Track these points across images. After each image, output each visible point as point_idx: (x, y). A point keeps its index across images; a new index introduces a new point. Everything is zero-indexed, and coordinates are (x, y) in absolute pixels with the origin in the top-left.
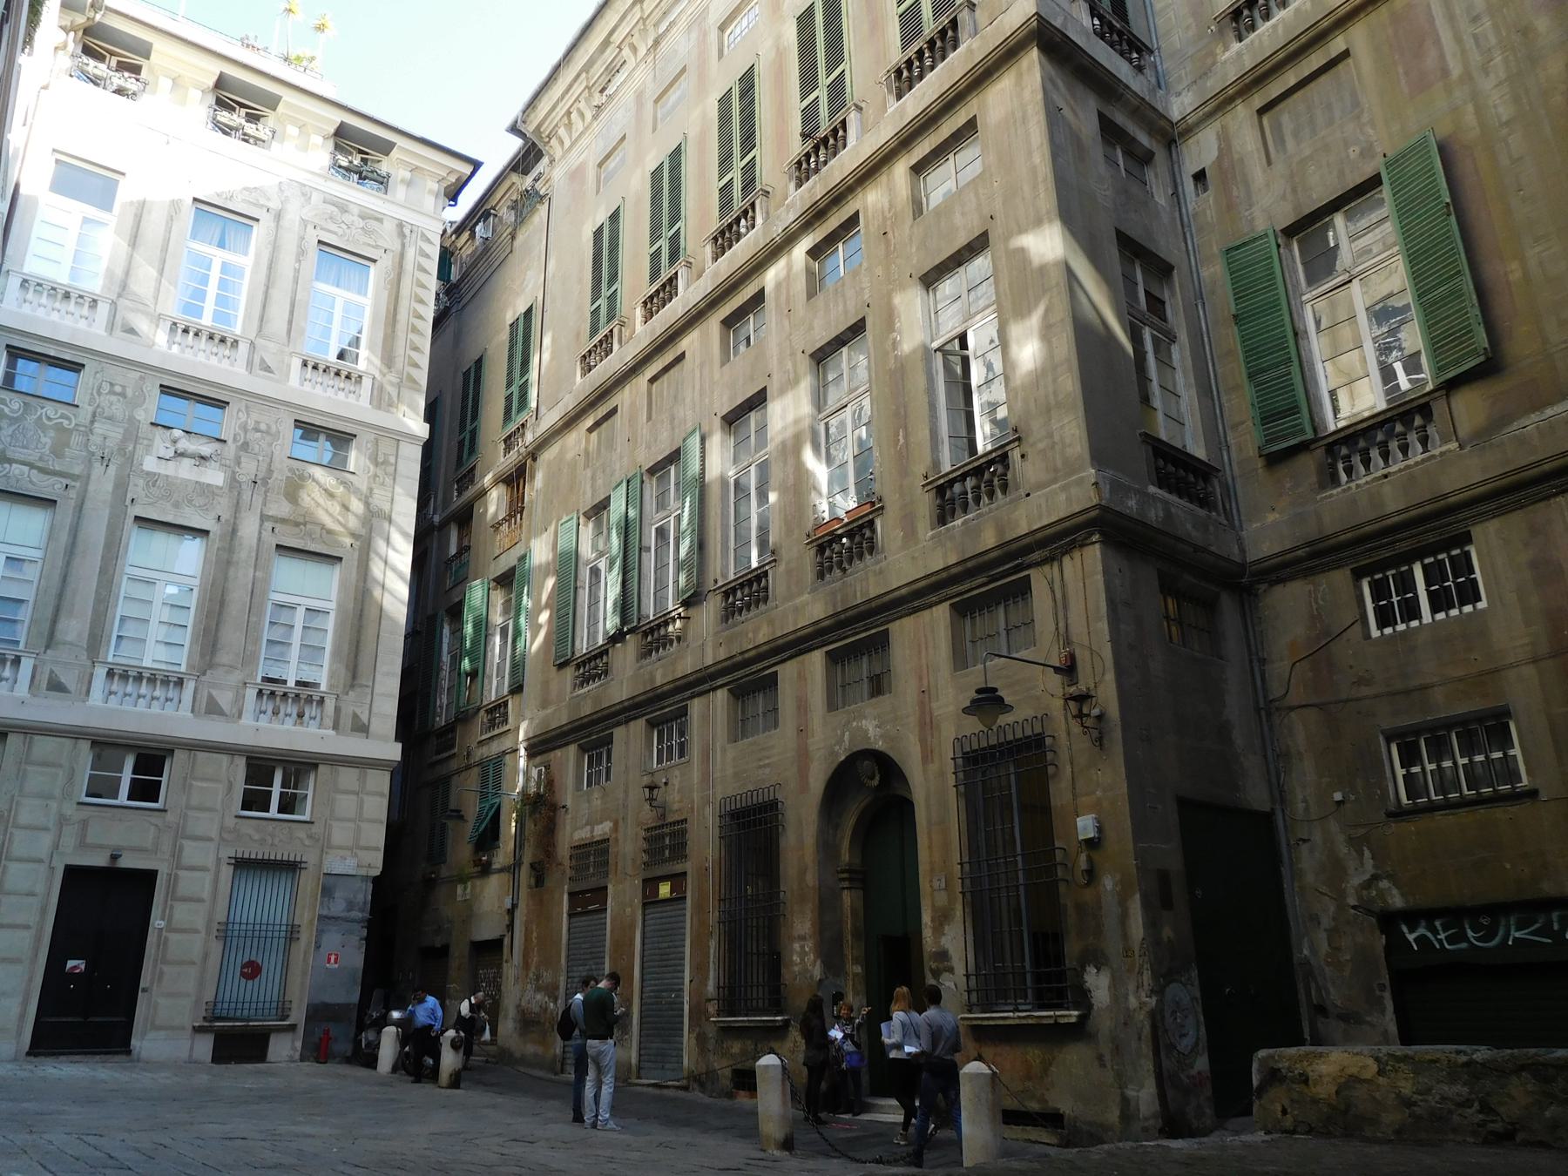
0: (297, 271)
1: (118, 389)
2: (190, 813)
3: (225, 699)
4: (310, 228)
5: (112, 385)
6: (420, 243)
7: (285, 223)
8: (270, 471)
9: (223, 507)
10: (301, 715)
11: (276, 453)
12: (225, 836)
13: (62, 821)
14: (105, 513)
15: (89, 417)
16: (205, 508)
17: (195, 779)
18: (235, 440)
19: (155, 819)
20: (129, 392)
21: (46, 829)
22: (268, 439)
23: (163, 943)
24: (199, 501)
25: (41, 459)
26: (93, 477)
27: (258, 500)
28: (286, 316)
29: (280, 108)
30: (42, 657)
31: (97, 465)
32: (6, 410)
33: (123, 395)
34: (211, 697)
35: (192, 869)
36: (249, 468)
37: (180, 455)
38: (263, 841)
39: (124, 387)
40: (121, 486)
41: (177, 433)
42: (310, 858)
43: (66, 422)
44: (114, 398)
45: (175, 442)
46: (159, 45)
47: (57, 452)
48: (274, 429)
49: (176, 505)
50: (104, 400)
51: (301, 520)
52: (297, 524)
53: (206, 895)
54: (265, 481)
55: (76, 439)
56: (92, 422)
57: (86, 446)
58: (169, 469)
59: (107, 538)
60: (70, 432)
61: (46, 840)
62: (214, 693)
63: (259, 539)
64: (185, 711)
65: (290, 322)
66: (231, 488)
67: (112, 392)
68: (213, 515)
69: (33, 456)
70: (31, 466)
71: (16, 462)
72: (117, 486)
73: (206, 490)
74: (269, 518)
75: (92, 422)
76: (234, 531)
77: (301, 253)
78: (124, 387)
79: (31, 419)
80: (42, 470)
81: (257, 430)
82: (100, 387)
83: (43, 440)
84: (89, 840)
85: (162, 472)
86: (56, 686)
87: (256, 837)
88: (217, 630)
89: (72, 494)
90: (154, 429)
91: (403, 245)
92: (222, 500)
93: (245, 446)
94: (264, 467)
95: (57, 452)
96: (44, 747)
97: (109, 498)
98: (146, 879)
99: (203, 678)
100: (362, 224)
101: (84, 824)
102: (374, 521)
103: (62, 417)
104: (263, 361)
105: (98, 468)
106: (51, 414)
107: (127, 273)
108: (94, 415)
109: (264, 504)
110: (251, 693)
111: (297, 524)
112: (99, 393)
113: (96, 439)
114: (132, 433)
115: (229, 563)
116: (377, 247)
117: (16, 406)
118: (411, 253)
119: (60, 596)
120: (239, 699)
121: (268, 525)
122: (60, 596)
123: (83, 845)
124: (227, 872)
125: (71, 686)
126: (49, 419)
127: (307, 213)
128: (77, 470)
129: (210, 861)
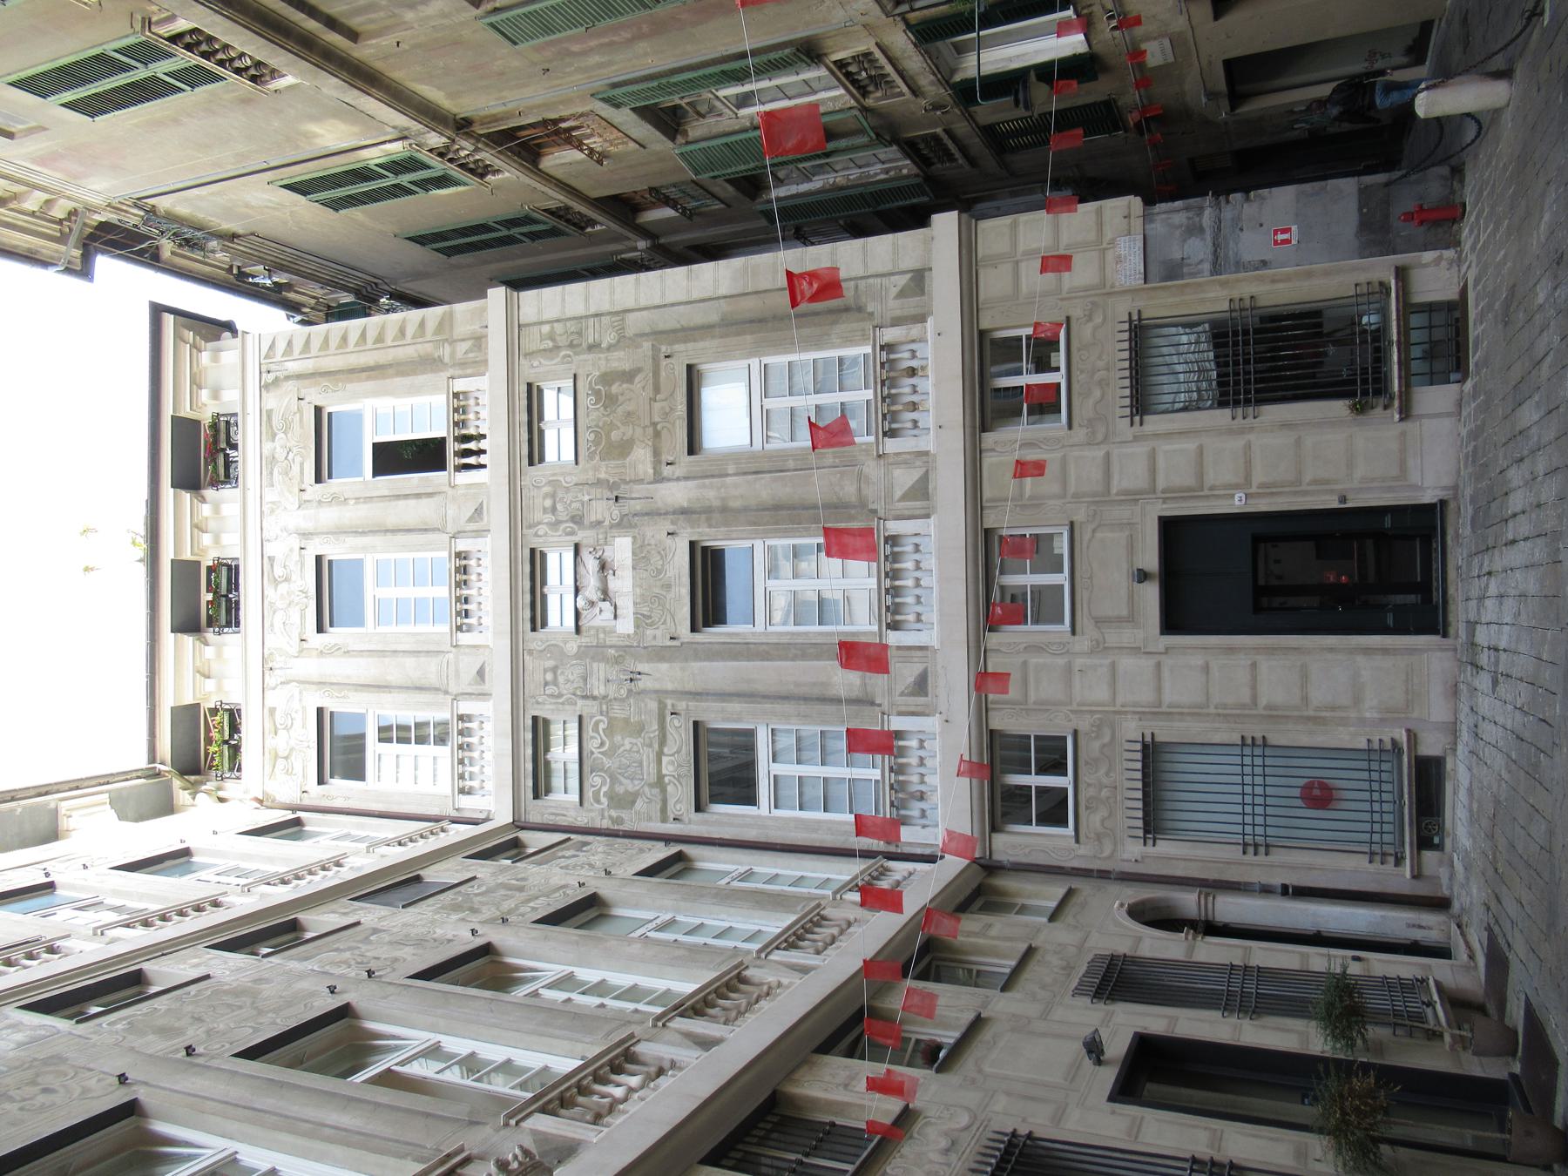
1: (549, 677)
2: (1072, 489)
3: (905, 478)
5: (546, 684)
6: (278, 358)
8: (599, 483)
9: (656, 531)
10: (912, 372)
11: (575, 480)
12: (1100, 437)
13: (1100, 648)
14: (696, 666)
17: (1021, 495)
18: (572, 533)
19: (1084, 536)
20: (550, 663)
21: (1113, 666)
22: (560, 494)
23: (1269, 489)
24: (656, 560)
25: (650, 746)
26: (657, 686)
27: (639, 490)
28: (412, 502)
29: (187, 556)
30: (885, 708)
31: (641, 685)
32: (605, 789)
33: (554, 670)
34: (904, 498)
35: (1153, 471)
36: (602, 510)
37: (606, 595)
38: (1103, 384)
40: (659, 654)
41: (581, 603)
42: (1122, 309)
43: (602, 726)
44: (561, 679)
45: (592, 604)
46: (168, 701)
47: (640, 729)
48: (547, 489)
49: (668, 587)
50: (566, 689)
51: (650, 430)
52: (657, 434)
53: (1190, 445)
54: (612, 486)
55: (618, 712)
56: (595, 698)
57: (623, 700)
58: (627, 605)
59: (723, 659)
60: (610, 720)
61: (1126, 663)
62: (898, 493)
63: (686, 478)
64: (929, 526)
65: (418, 496)
66: (631, 526)
68: (669, 541)
69: (648, 756)
70: (660, 755)
71: (659, 770)
72: (662, 659)
73: (641, 557)
74: (657, 472)
75: (595, 698)
76: (684, 512)
77: (336, 500)
78: (545, 671)
79: (607, 763)
80: (663, 742)
81: (554, 509)
82: (552, 696)
83: (628, 747)
84: (1125, 613)
85: (631, 610)
86: (921, 685)
87: (1097, 393)
89: (681, 706)
90: (583, 629)
91: (287, 378)
93: (577, 520)
94: (598, 492)
95: (640, 729)
97: (677, 665)
98: (1170, 528)
99: (881, 513)
100: (281, 435)
101: (1100, 622)
102: (630, 332)
103: (596, 729)
104: (470, 520)
105: (644, 683)
106: (596, 743)
108: (585, 697)
109: (641, 481)
110: (891, 446)
111: (657, 434)
112: (560, 695)
113: (612, 691)
114: (595, 652)
115: (724, 510)
117: (598, 780)
118: (293, 367)
119: (806, 699)
120: (903, 460)
121: (667, 471)
122: (806, 699)
123: (1131, 619)
124: (1154, 423)
126: (602, 744)
127: (292, 500)
129: (1141, 449)
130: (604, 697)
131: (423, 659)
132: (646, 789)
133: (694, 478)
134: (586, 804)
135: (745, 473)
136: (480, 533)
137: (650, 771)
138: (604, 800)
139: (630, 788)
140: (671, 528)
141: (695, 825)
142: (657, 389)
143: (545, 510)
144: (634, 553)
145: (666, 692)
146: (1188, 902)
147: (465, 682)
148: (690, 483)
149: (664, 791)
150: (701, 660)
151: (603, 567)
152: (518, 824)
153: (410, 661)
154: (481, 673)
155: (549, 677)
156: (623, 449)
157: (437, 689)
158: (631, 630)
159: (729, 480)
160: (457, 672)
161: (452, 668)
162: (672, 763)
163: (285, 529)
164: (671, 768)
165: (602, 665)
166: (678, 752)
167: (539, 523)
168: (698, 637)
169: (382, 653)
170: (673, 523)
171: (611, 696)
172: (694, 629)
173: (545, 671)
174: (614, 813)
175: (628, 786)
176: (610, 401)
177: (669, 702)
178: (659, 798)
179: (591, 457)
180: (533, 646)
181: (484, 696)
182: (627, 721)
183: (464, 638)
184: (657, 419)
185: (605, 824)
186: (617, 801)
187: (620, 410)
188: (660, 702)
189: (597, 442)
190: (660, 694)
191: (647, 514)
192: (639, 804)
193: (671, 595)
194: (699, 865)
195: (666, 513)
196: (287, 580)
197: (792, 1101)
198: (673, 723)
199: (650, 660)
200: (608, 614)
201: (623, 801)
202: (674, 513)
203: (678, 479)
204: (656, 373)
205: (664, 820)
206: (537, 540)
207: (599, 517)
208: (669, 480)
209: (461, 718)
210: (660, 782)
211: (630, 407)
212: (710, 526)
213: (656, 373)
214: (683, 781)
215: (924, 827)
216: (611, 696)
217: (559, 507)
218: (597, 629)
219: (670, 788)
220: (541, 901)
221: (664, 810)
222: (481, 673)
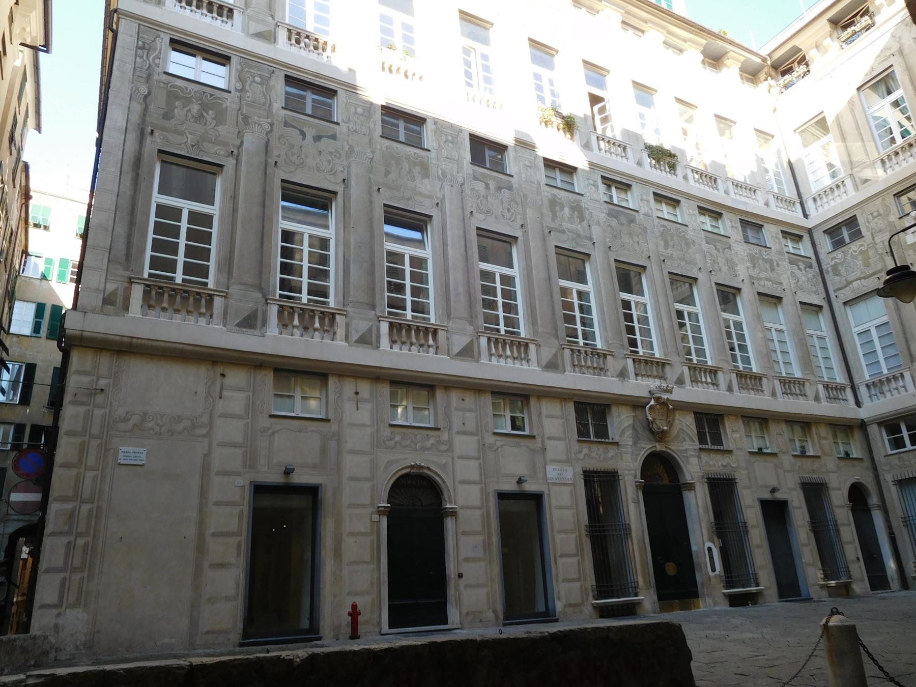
1: (875, 214)
7: (906, 51)
15: (871, 237)
20: (881, 211)
30: (912, 368)
33: (880, 215)
39: (877, 211)
44: (876, 220)
50: (873, 225)
55: (871, 253)
60: (866, 251)
67: (874, 218)
69: (858, 274)
70: (860, 279)
79: (848, 257)
80: (866, 278)
95: (867, 265)
106: (855, 249)
107: (849, 156)
108: (872, 235)
112: (869, 223)
117: (840, 256)
137: (851, 277)
139: (842, 272)
146: (874, 500)
149: (846, 286)
152: (810, 231)
154: (866, 181)
158: (909, 243)
169: (858, 128)
173: (877, 211)
174: (830, 269)
175: (842, 270)
178: (842, 285)
181: (856, 187)
185: (824, 267)
186: (835, 268)
192: (837, 278)
194: (821, 316)
197: (723, 420)
201: (835, 270)
210: (849, 283)
215: (870, 397)
220: (769, 284)
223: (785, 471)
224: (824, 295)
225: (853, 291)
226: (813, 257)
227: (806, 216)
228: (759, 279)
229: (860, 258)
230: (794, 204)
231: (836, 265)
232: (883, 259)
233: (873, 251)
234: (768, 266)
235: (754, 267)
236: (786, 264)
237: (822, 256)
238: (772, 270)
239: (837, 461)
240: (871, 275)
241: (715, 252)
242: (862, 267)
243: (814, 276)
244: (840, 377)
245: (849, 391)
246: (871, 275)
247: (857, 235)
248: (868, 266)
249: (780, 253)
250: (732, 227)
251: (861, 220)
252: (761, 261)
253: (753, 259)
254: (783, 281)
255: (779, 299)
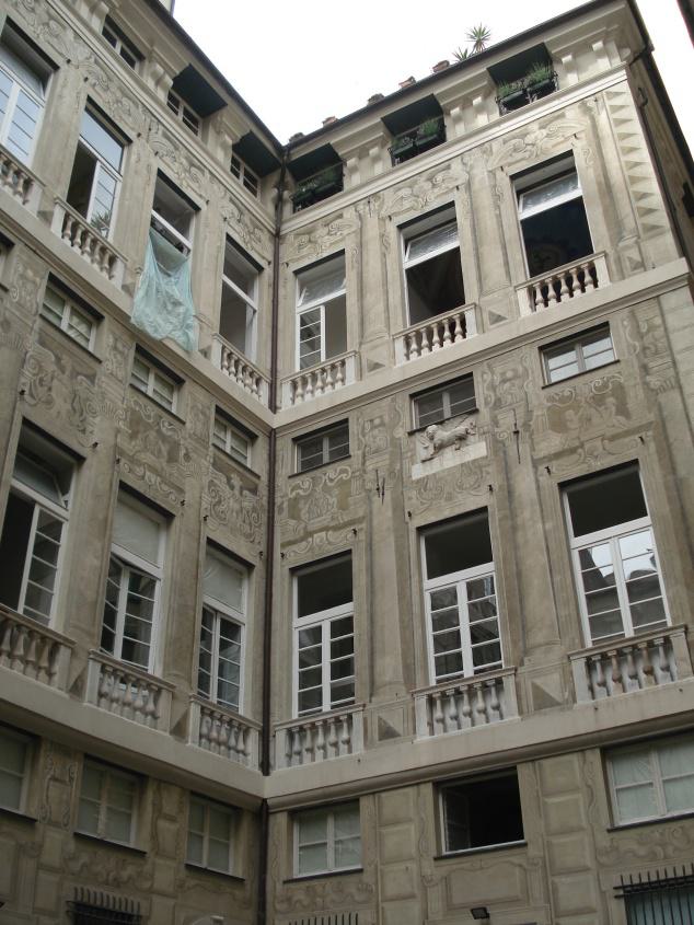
0: (499, 216)
1: (377, 421)
2: (555, 840)
3: (552, 685)
4: (499, 174)
6: (608, 103)
7: (476, 186)
8: (529, 412)
10: (650, 672)
12: (603, 860)
14: (392, 539)
16: (476, 486)
18: (486, 403)
20: (386, 419)
21: (412, 896)
22: (517, 382)
24: (472, 480)
25: (333, 519)
26: (375, 511)
27: (525, 448)
28: (501, 260)
31: (376, 498)
33: (382, 424)
34: (536, 688)
36: (507, 421)
37: (440, 448)
38: (653, 856)
39: (381, 417)
44: (376, 432)
45: (432, 438)
48: (520, 369)
49: (450, 498)
50: (368, 439)
51: (577, 443)
52: (573, 451)
54: (526, 425)
55: (355, 485)
56: (364, 464)
57: (363, 486)
58: (435, 467)
62: (538, 682)
63: (538, 488)
64: (512, 717)
65: (507, 263)
66: (496, 452)
67: (374, 427)
69: (325, 520)
70: (326, 529)
71: (316, 532)
73: (475, 467)
75: (364, 464)
77: (497, 197)
79: (319, 489)
80: (336, 528)
81: (504, 381)
82: (363, 428)
83: (331, 502)
87: (642, 851)
88: (522, 608)
91: (593, 119)
92: (490, 469)
94: (521, 412)
95: (343, 507)
96: (393, 801)
100: (544, 132)
101: (447, 880)
102: (662, 398)
104: (491, 314)
105: (377, 500)
106: (332, 476)
108: (364, 456)
109: (533, 449)
110: (579, 667)
111: (573, 451)
113: (370, 476)
114: (398, 454)
115: (514, 529)
116: (567, 139)
118: (603, 119)
120: (568, 676)
121: (542, 468)
125: (398, 728)
126: (331, 480)
127: (494, 163)
128: (361, 514)
129: (594, 899)
130: (365, 471)
131: (383, 316)
132: (303, 525)
133: (539, 495)
134: (291, 481)
135: (546, 539)
136: (481, 328)
137: (315, 524)
138: (294, 494)
140: (495, 488)
141: (281, 571)
142: (613, 438)
143: (503, 374)
144: (474, 461)
145: (371, 520)
147: (369, 355)
148: (535, 492)
149: (303, 539)
150: (396, 541)
151: (462, 438)
152: (272, 434)
153: (381, 307)
154: (376, 366)
155: (377, 421)
156: (559, 425)
157: (362, 336)
158: (414, 478)
159: (540, 525)
160: (376, 347)
161: (379, 341)
162: (321, 541)
163: (472, 167)
164: (318, 540)
165: (387, 462)
166: (330, 543)
167: (493, 373)
168: (413, 535)
169: (385, 283)
170: (500, 487)
171: (366, 476)
172: (420, 530)
173: (381, 417)
174: (285, 505)
175: (304, 508)
176: (598, 400)
177: (364, 525)
179: (551, 399)
180: (399, 401)
181: (360, 375)
182: (349, 495)
183: (400, 345)
184: (587, 446)
185: (278, 500)
187: (593, 410)
188: (364, 517)
189: (563, 399)
190: (368, 517)
191: (506, 463)
192: (292, 522)
193: (443, 502)
195: (508, 479)
196: (434, 186)
198: (347, 533)
199: (392, 499)
200: (424, 454)
202: (509, 486)
203: (537, 481)
204: (628, 433)
205: (283, 546)
206: (479, 374)
207: (501, 422)
208: (536, 473)
209: (343, 363)
210: (310, 534)
211: (596, 420)
212: (500, 520)
213: (628, 433)
214: (310, 554)
216: (366, 476)
217: (507, 385)
218: (414, 449)
219: (304, 543)
220: (154, 479)
221: (290, 543)
222: (376, 366)
223: (40, 867)
224: (263, 547)
225: (312, 549)
226: (264, 478)
227: (273, 407)
228: (133, 460)
229: (336, 491)
230: (258, 382)
231: (297, 499)
232: (369, 498)
233: (359, 482)
234: (164, 449)
235: (133, 436)
236: (206, 463)
237: (281, 481)
238: (172, 459)
239: (183, 873)
240: (346, 525)
241: (51, 367)
242: (335, 509)
243: (254, 509)
244: (246, 706)
245: (254, 737)
246: (346, 525)
247: (342, 454)
248: (344, 510)
249: (202, 440)
250: (115, 348)
251: (353, 428)
252: (152, 434)
253: (136, 424)
254: (187, 488)
255: (168, 517)
